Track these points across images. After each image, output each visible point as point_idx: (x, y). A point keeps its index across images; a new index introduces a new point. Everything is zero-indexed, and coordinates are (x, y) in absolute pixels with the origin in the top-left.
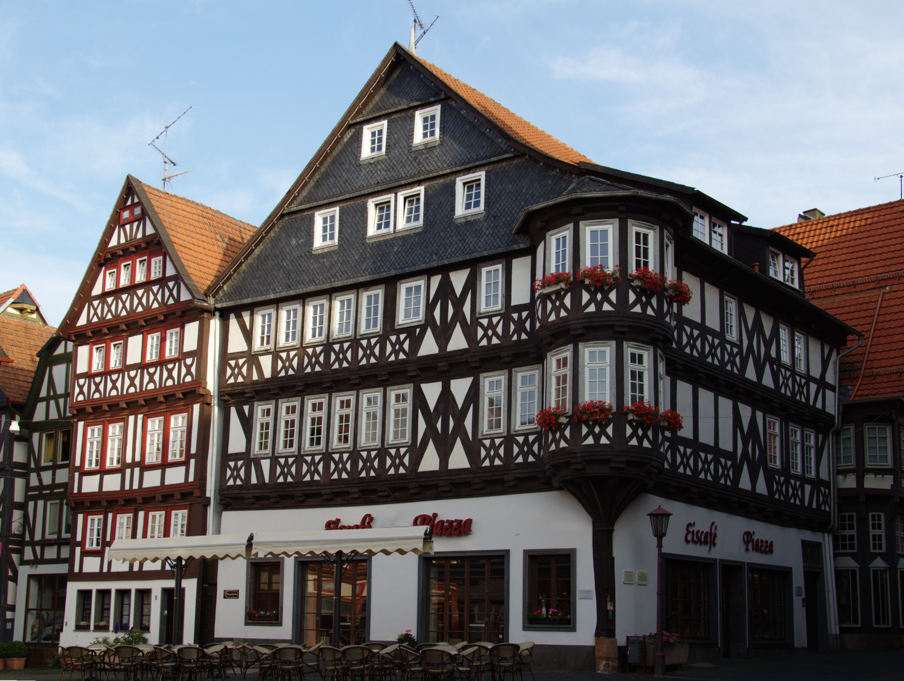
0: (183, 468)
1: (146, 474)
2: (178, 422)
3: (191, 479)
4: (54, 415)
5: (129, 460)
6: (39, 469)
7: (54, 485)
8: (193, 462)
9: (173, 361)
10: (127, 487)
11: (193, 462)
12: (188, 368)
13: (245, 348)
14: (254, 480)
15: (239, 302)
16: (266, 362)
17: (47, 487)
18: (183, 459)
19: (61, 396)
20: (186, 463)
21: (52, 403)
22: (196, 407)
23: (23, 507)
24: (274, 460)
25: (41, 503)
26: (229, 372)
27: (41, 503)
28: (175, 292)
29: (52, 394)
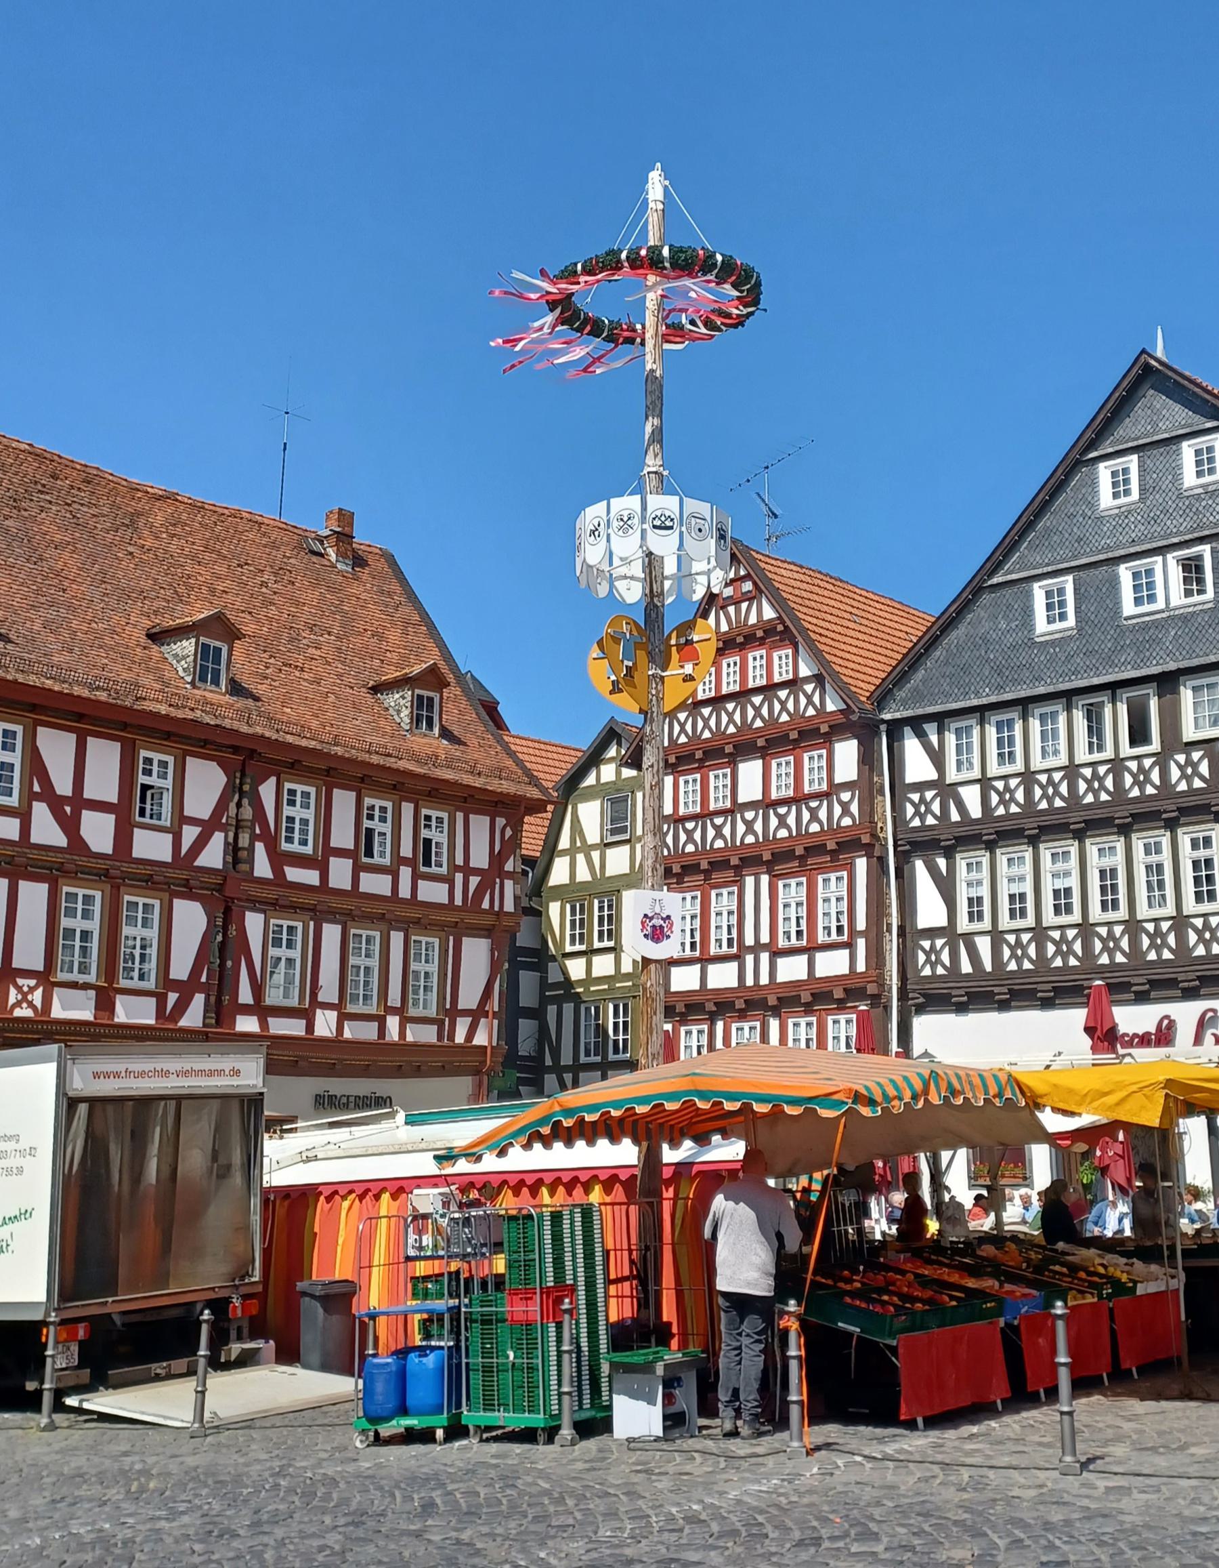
0: (845, 953)
1: (781, 962)
2: (831, 887)
3: (861, 967)
4: (583, 875)
5: (749, 941)
8: (861, 943)
9: (818, 796)
10: (750, 982)
11: (861, 943)
12: (845, 807)
13: (931, 774)
14: (966, 967)
15: (920, 712)
16: (971, 797)
18: (845, 938)
19: (594, 847)
20: (850, 945)
21: (580, 858)
22: (861, 864)
24: (997, 936)
26: (910, 810)
28: (816, 699)
29: (579, 844)
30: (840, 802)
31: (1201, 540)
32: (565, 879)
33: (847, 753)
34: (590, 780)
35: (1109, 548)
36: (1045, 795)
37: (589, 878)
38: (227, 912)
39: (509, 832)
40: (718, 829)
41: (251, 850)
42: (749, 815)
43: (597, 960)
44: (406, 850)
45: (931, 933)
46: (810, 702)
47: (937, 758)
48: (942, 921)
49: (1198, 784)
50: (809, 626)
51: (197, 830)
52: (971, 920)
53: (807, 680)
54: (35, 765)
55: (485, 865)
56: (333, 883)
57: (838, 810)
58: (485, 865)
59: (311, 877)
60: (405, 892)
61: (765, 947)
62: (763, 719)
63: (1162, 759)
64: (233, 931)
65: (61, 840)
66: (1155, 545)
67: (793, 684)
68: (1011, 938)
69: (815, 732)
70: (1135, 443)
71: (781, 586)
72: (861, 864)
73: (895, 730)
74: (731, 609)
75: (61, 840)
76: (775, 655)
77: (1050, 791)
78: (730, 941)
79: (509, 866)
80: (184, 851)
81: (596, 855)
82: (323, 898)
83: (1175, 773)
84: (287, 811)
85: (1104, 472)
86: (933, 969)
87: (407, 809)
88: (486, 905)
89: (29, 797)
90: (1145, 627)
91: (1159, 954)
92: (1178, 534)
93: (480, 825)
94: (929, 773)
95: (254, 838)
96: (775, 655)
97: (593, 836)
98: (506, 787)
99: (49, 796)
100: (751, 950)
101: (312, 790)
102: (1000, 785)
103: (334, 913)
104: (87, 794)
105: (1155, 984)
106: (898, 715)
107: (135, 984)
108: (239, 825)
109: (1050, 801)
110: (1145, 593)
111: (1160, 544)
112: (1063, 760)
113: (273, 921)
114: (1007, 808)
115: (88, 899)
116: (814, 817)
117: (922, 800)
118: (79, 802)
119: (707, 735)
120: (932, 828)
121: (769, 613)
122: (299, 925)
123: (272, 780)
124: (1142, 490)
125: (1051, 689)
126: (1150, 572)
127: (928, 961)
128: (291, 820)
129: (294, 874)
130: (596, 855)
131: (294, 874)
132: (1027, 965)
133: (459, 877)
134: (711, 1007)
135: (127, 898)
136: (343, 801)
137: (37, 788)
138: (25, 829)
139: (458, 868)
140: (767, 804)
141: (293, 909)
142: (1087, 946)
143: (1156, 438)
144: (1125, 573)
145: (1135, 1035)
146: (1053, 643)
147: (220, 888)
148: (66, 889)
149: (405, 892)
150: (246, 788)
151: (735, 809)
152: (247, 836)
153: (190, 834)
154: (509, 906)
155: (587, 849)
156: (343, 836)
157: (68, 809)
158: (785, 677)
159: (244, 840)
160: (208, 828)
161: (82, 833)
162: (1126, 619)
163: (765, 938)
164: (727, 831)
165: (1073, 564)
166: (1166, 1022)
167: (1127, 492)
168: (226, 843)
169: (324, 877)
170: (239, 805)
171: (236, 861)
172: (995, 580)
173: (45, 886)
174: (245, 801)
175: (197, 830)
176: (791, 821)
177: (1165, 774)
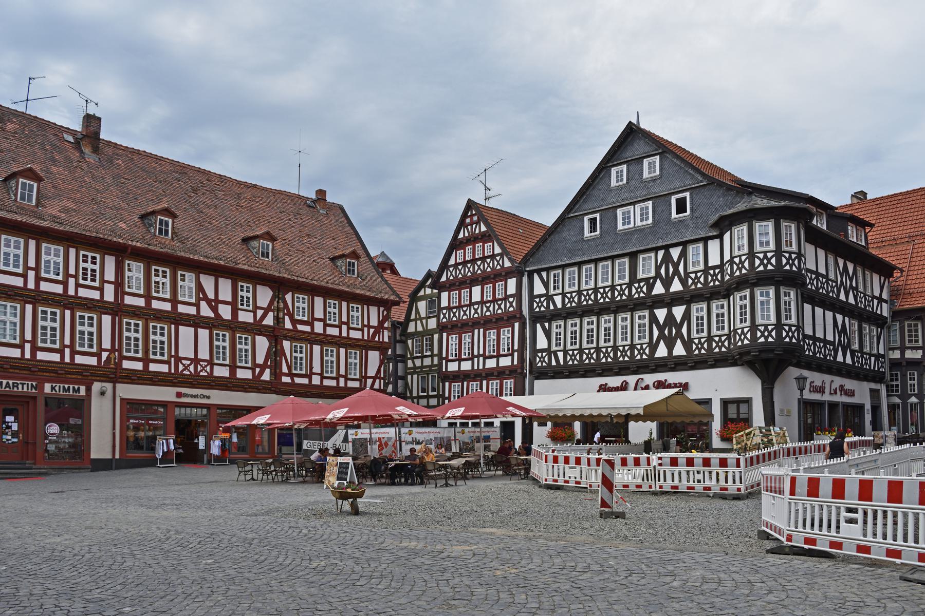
0: (510, 358)
1: (487, 361)
2: (505, 333)
3: (515, 363)
4: (420, 329)
5: (476, 353)
6: (413, 358)
7: (422, 367)
8: (516, 354)
9: (501, 299)
10: (476, 368)
11: (516, 354)
12: (511, 303)
13: (544, 292)
14: (554, 363)
15: (540, 267)
16: (558, 300)
17: (418, 368)
18: (510, 352)
19: (424, 318)
20: (512, 355)
21: (419, 322)
22: (517, 325)
23: (404, 378)
24: (565, 352)
25: (415, 376)
26: (535, 305)
27: (415, 376)
28: (501, 262)
30: (509, 302)
31: (648, 199)
32: (413, 330)
33: (512, 283)
34: (422, 293)
35: (613, 203)
36: (585, 299)
37: (422, 330)
38: (276, 341)
39: (385, 313)
40: (465, 312)
41: (284, 318)
42: (476, 307)
43: (425, 360)
44: (344, 319)
45: (542, 351)
46: (498, 263)
47: (546, 285)
48: (546, 346)
49: (642, 295)
50: (499, 234)
51: (262, 311)
52: (556, 346)
53: (498, 255)
54: (200, 288)
55: (376, 324)
56: (316, 331)
57: (508, 305)
58: (376, 324)
59: (307, 329)
60: (344, 334)
61: (481, 356)
62: (481, 270)
63: (630, 286)
64: (279, 347)
65: (212, 315)
66: (631, 201)
67: (493, 257)
68: (571, 353)
69: (500, 275)
70: (625, 160)
71: (489, 218)
72: (517, 325)
73: (530, 275)
74: (469, 227)
75: (212, 315)
76: (486, 245)
77: (587, 297)
78: (469, 353)
79: (386, 325)
80: (258, 319)
81: (424, 321)
82: (312, 336)
83: (634, 291)
84: (296, 304)
85: (614, 171)
86: (542, 364)
87: (344, 304)
88: (377, 339)
89: (199, 299)
90: (626, 234)
91: (624, 358)
92: (640, 197)
93: (374, 310)
94: (543, 291)
95: (284, 314)
96: (486, 245)
97: (423, 313)
98: (385, 296)
99: (206, 299)
100: (476, 356)
101: (306, 297)
102: (569, 295)
103: (317, 341)
104: (220, 298)
105: (604, 370)
106: (531, 268)
107: (243, 364)
108: (278, 310)
109: (587, 302)
110: (626, 220)
111: (633, 201)
112: (610, 283)
113: (293, 344)
114: (571, 304)
115: (224, 335)
116: (500, 308)
117: (540, 301)
118: (217, 301)
119: (460, 276)
120: (543, 311)
121: (483, 228)
122: (304, 346)
123: (290, 294)
124: (628, 179)
125: (589, 258)
126: (629, 212)
127: (540, 361)
128: (298, 308)
129: (300, 327)
130: (424, 321)
131: (300, 327)
132: (576, 362)
133: (366, 329)
134: (462, 376)
135: (238, 335)
136: (319, 301)
137: (201, 296)
138: (198, 310)
139: (365, 326)
140: (482, 302)
141: (301, 340)
142: (598, 356)
143: (634, 158)
144: (619, 212)
145: (613, 388)
146: (590, 240)
147: (273, 332)
148: (215, 332)
149: (344, 334)
150: (280, 296)
151: (471, 304)
152: (282, 313)
153: (260, 313)
154: (386, 340)
155: (421, 319)
156: (319, 314)
157: (213, 304)
158: (489, 254)
159: (281, 315)
160: (267, 311)
161: (219, 312)
162: (619, 231)
163: (481, 352)
164: (468, 313)
165: (599, 209)
166: (624, 383)
167: (622, 180)
168: (274, 316)
169: (313, 328)
170: (278, 302)
171: (278, 323)
172: (570, 216)
173: (208, 331)
174: (280, 301)
175: (262, 311)
176: (491, 309)
177: (630, 291)
